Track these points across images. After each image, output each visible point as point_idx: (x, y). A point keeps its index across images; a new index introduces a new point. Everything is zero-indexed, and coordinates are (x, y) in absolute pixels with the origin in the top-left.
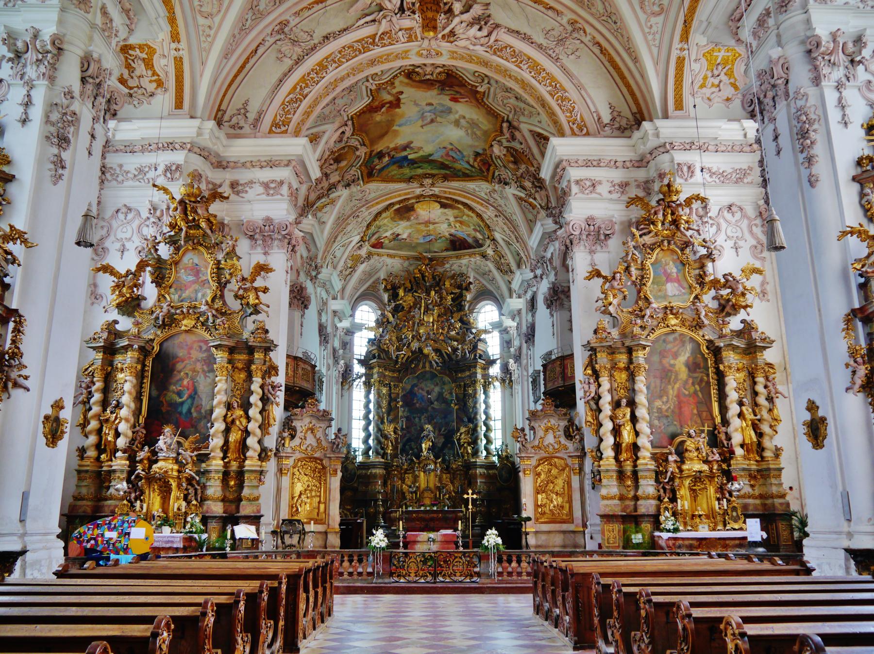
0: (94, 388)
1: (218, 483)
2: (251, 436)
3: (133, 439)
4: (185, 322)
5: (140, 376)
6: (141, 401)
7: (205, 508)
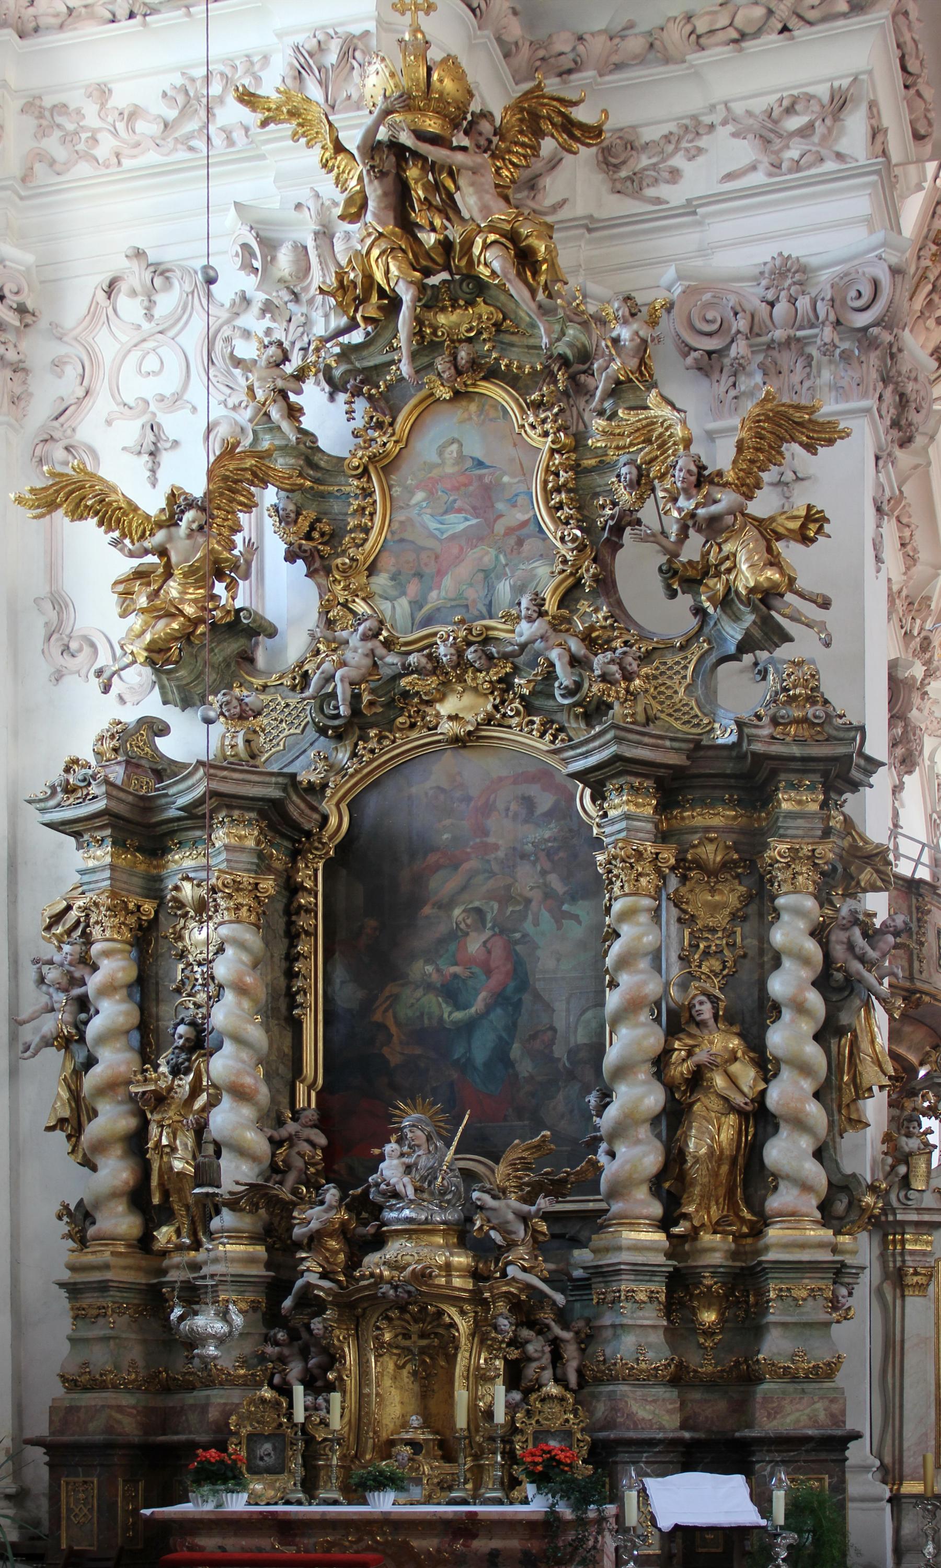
0: (94, 982)
1: (651, 1316)
2: (785, 1131)
3: (274, 1168)
4: (445, 709)
5: (282, 924)
6: (296, 1026)
7: (601, 1409)
